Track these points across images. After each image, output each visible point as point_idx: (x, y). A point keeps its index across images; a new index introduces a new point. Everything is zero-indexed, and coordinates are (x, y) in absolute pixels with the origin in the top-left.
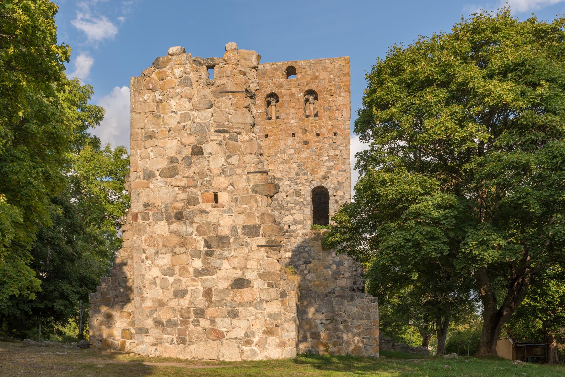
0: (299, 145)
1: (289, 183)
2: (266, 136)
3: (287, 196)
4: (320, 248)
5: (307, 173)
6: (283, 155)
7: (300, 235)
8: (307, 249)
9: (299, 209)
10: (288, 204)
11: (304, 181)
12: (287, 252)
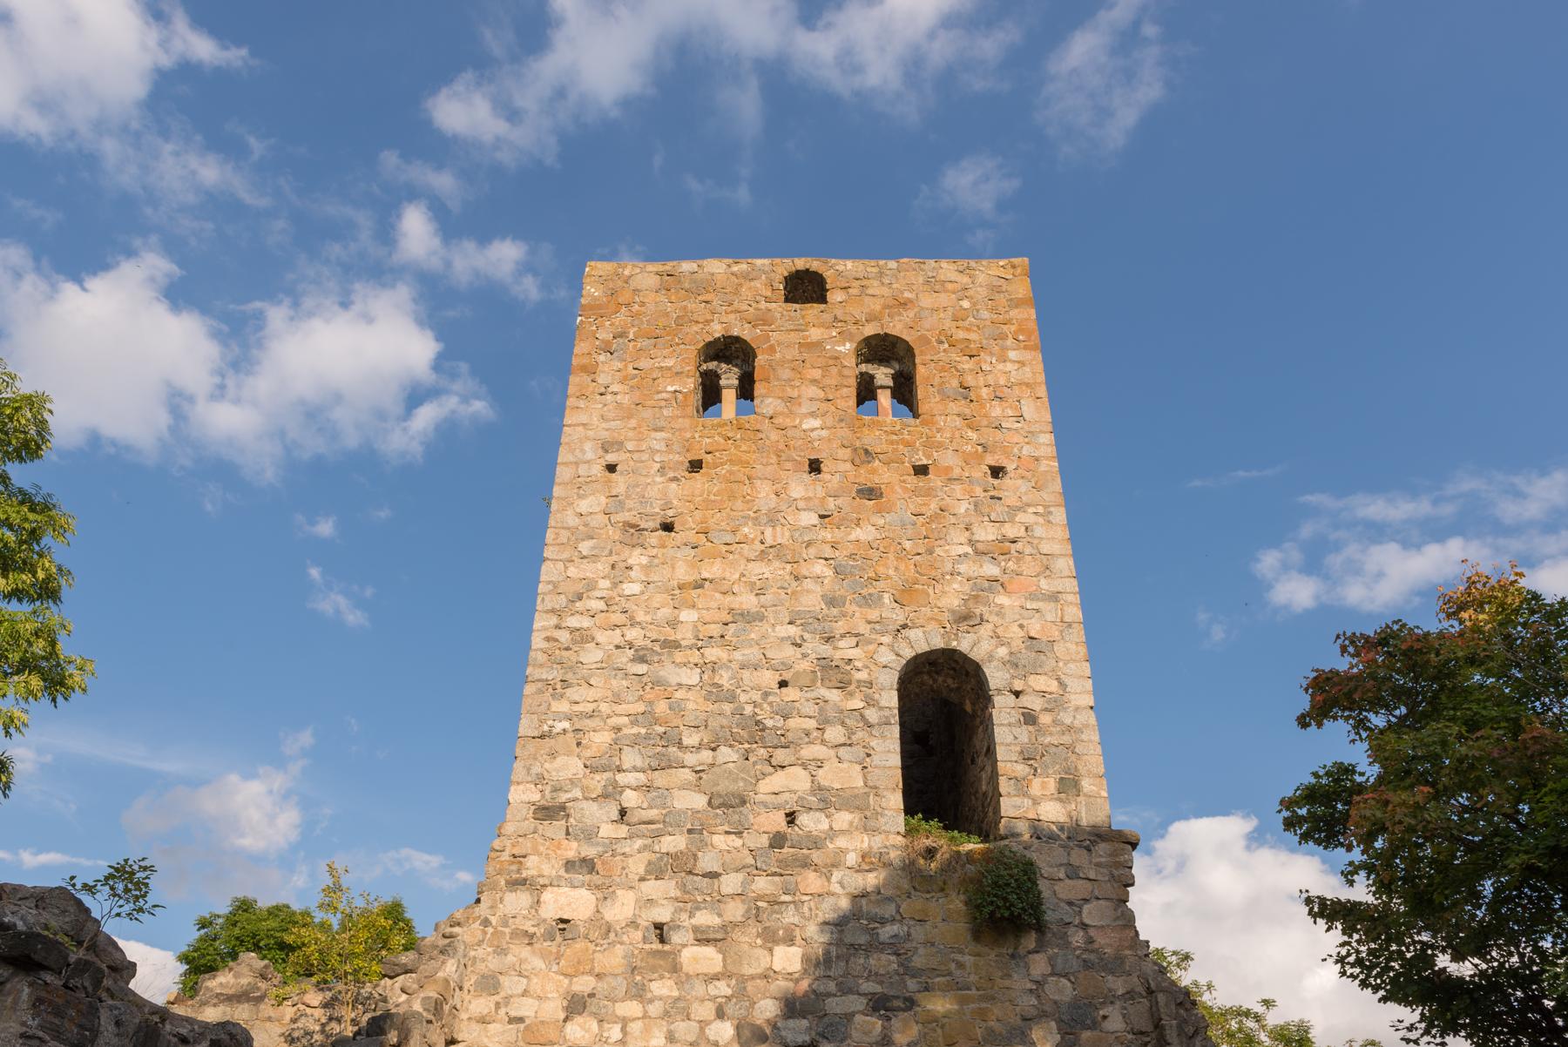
0: (839, 502)
1: (793, 631)
2: (696, 466)
3: (783, 684)
4: (962, 927)
5: (880, 598)
6: (768, 532)
7: (852, 859)
8: (886, 932)
9: (842, 740)
10: (786, 717)
11: (863, 628)
12: (776, 942)
